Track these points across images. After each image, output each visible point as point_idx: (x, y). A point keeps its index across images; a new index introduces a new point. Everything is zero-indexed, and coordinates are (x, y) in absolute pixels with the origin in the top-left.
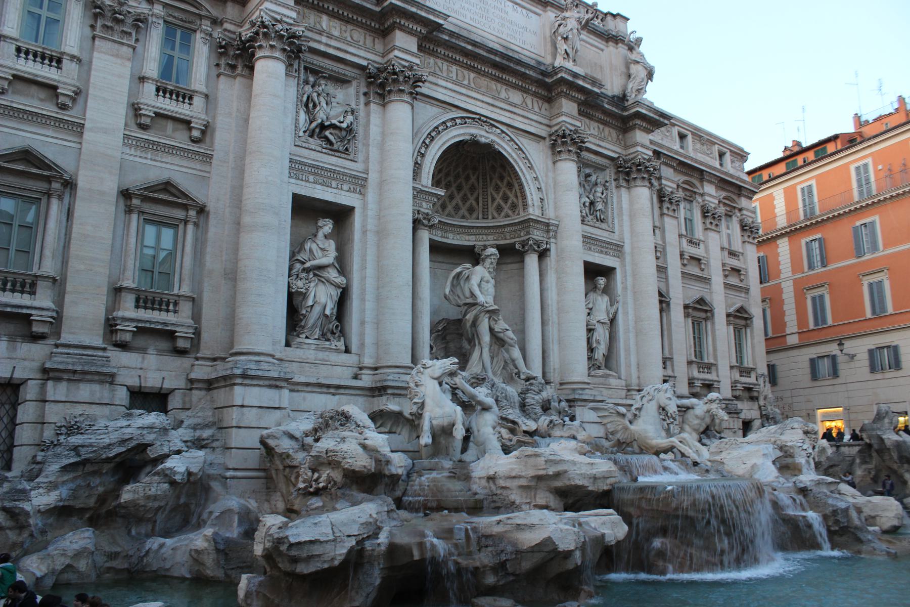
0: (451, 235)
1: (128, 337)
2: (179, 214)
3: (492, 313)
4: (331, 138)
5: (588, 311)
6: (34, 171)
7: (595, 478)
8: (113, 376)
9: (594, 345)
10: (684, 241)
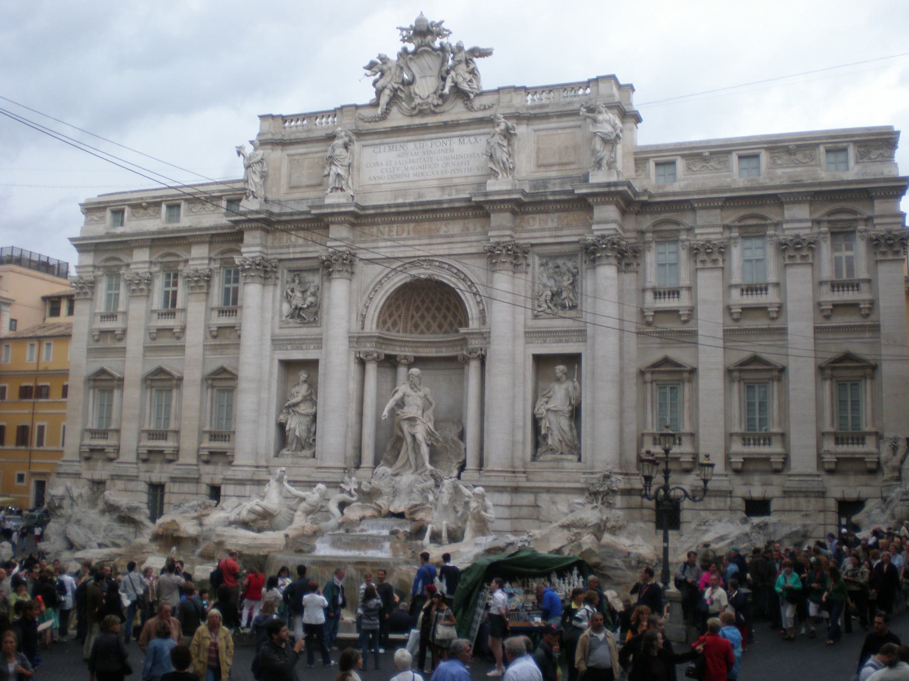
0: (444, 349)
1: (205, 458)
2: (231, 383)
3: (412, 420)
4: (304, 315)
5: (545, 399)
6: (163, 377)
7: (248, 547)
8: (198, 479)
9: (543, 432)
10: (735, 294)
